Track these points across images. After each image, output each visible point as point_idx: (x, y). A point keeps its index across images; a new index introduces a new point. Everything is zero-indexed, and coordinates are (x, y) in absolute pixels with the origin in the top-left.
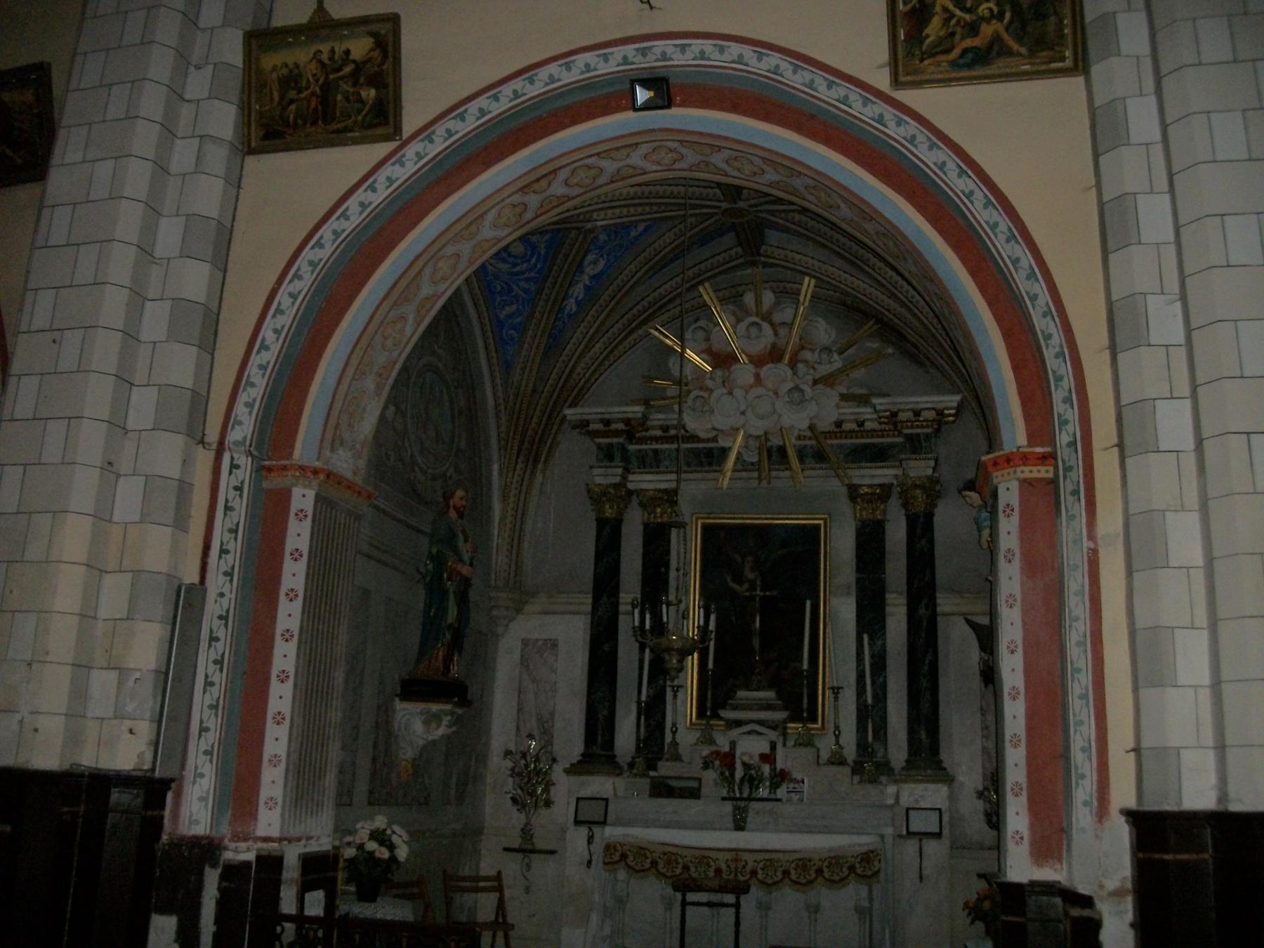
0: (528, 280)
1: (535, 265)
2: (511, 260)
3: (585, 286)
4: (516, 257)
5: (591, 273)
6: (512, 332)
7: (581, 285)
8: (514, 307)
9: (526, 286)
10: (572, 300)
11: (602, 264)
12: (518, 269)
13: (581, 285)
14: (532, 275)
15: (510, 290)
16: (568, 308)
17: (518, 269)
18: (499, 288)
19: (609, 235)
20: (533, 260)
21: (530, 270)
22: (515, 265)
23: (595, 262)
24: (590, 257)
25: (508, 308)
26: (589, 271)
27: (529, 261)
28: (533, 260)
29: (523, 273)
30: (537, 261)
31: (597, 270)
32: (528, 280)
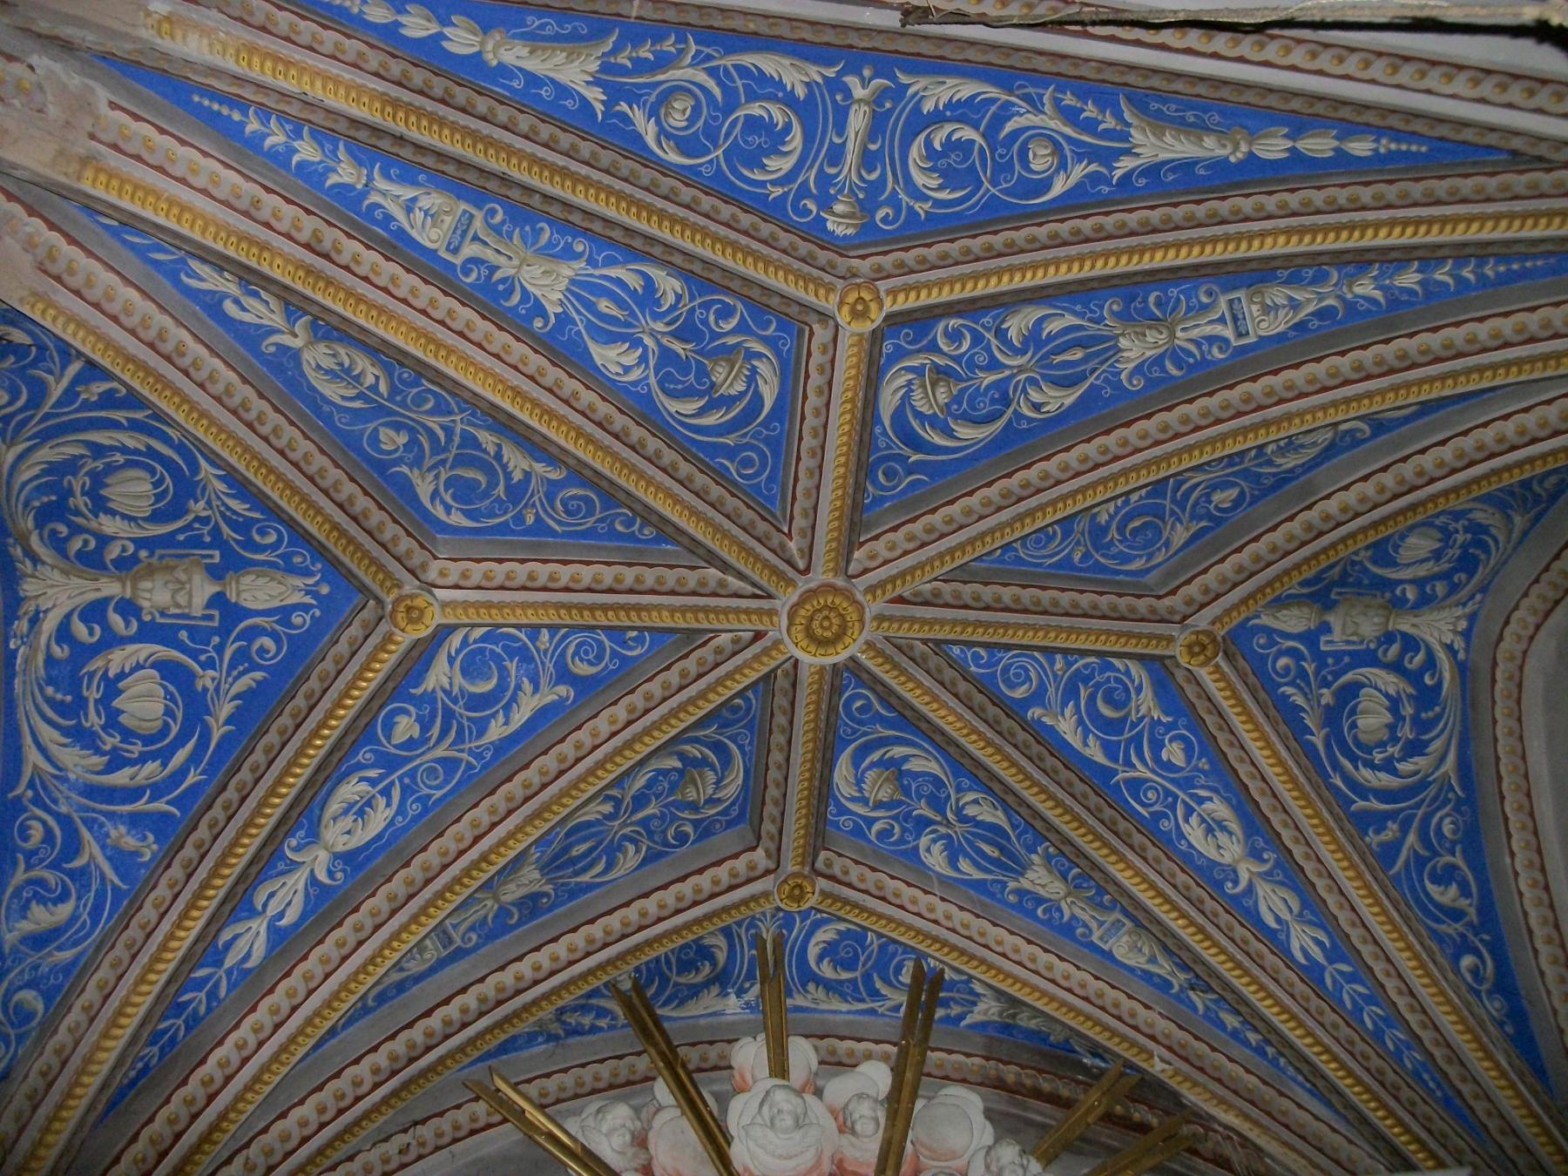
0: (135, 821)
1: (182, 773)
2: (111, 741)
3: (313, 880)
4: (128, 734)
5: (343, 844)
6: (29, 997)
7: (298, 880)
8: (64, 910)
9: (130, 842)
10: (259, 926)
11: (379, 818)
12: (121, 778)
13: (298, 880)
14: (161, 806)
15: (73, 846)
16: (241, 947)
17: (121, 778)
18: (37, 832)
19: (425, 727)
20: (181, 756)
21: (157, 791)
22: (116, 762)
23: (361, 810)
24: (352, 789)
25: (37, 911)
26: (340, 835)
27: (165, 756)
28: (181, 756)
29: (133, 794)
30: (194, 758)
31: (362, 837)
32: (135, 822)
